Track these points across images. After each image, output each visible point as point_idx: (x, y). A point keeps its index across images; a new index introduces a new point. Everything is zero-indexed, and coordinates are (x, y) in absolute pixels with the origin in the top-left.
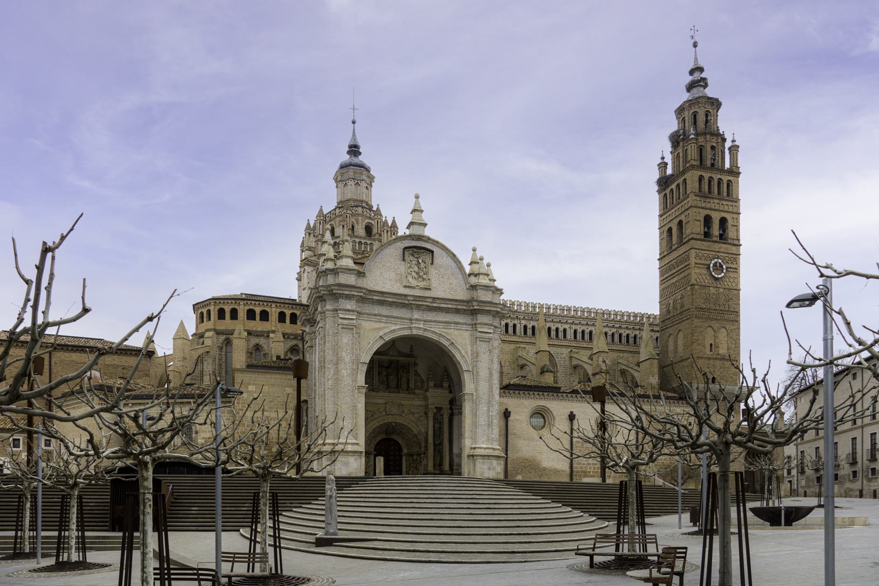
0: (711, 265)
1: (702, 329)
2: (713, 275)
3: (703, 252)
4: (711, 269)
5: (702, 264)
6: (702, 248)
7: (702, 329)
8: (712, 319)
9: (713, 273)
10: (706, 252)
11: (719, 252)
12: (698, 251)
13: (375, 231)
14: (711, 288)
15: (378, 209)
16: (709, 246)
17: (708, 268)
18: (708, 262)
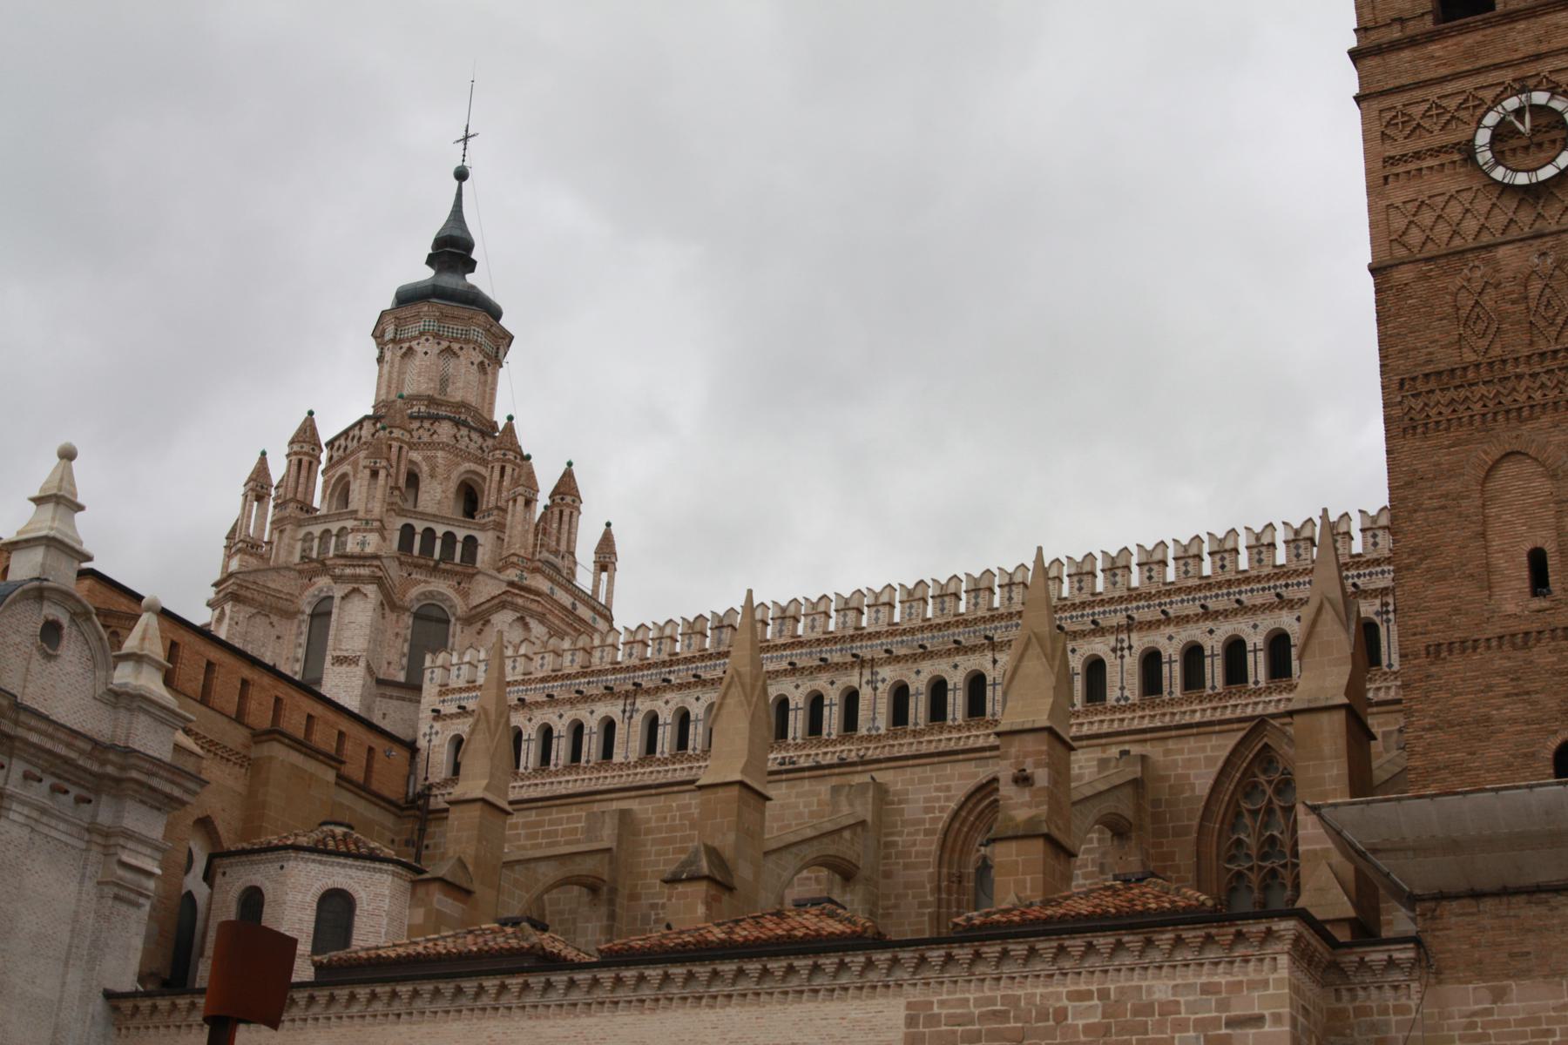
0: (1483, 137)
1: (1452, 486)
2: (1506, 189)
3: (1433, 93)
4: (1485, 157)
5: (1436, 152)
6: (1423, 77)
7: (1452, 486)
8: (1517, 414)
9: (1499, 173)
10: (1450, 88)
11: (1538, 57)
12: (1398, 101)
13: (488, 499)
14: (1502, 252)
15: (509, 428)
16: (1469, 54)
17: (1468, 150)
18: (1457, 135)
